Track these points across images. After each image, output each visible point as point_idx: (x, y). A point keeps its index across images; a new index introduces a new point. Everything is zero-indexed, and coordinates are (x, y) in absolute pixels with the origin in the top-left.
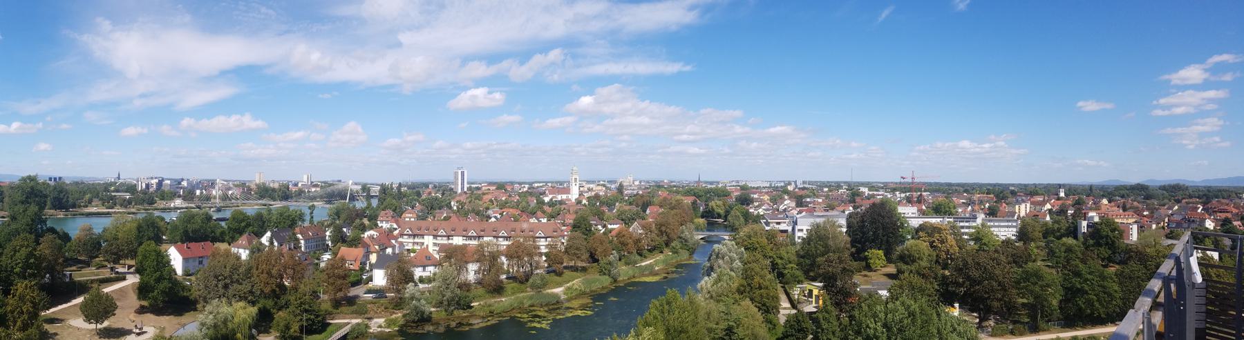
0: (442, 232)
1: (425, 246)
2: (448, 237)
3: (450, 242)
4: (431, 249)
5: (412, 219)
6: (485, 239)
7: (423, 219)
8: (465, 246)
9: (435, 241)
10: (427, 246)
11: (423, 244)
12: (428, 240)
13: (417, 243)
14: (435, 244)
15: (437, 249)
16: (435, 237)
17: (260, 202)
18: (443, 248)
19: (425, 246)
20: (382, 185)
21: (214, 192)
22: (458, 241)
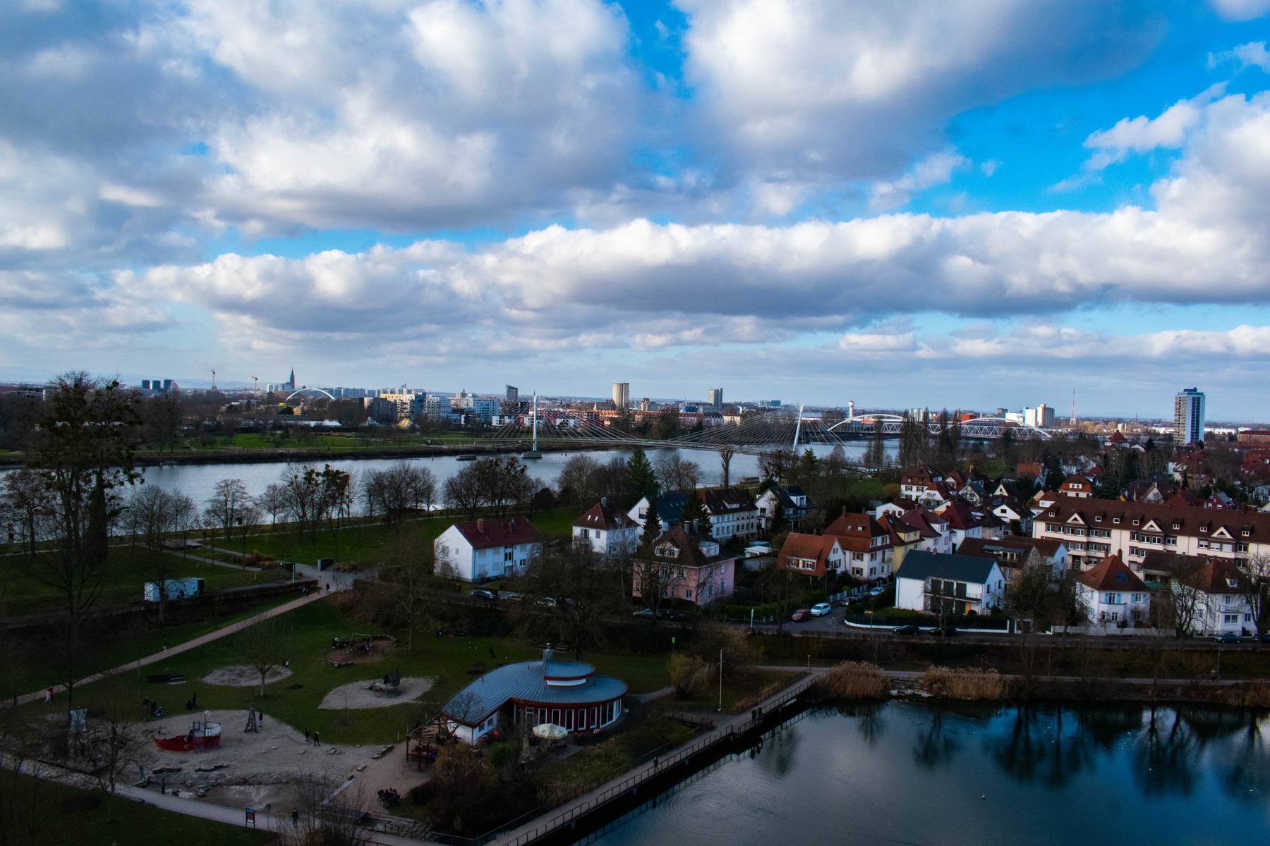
0: (1152, 526)
1: (1114, 552)
2: (1167, 537)
3: (1171, 547)
4: (1126, 559)
5: (1083, 495)
6: (1253, 548)
7: (1107, 497)
8: (1202, 558)
9: (1136, 544)
10: (1120, 552)
11: (1109, 545)
12: (1120, 541)
13: (1099, 546)
14: (1133, 550)
15: (1141, 560)
16: (1137, 534)
17: (624, 441)
18: (1153, 560)
19: (1114, 552)
20: (905, 414)
21: (527, 421)
22: (1187, 546)
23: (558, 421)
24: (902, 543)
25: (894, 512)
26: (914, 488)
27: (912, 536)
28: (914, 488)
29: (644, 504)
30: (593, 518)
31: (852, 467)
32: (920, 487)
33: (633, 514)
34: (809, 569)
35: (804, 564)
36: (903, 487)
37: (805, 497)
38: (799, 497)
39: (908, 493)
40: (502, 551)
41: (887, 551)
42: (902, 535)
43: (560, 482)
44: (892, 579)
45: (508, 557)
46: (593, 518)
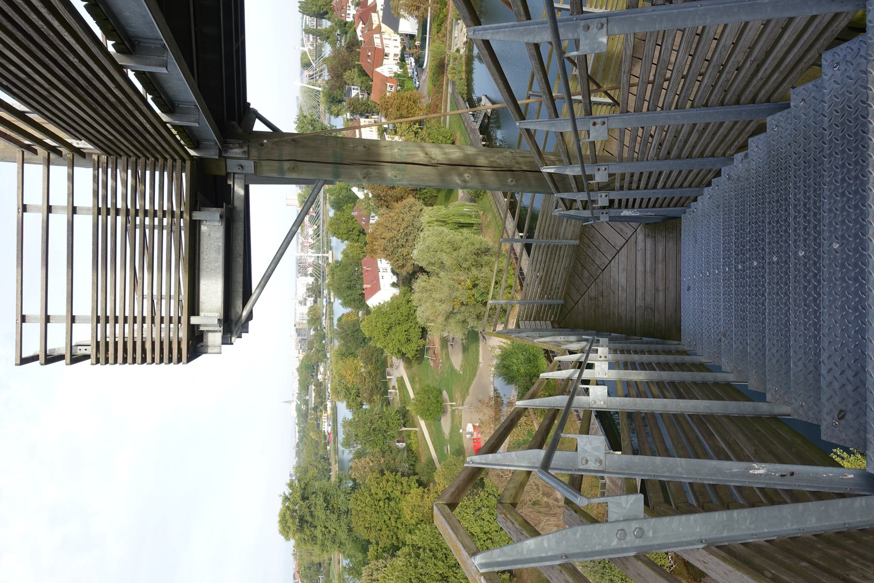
23: (311, 241)
24: (379, 27)
25: (362, 28)
26: (348, 12)
27: (374, 16)
28: (348, 12)
29: (355, 190)
30: (364, 221)
31: (336, 53)
32: (348, 8)
33: (360, 195)
34: (393, 88)
35: (391, 89)
36: (348, 20)
37: (352, 87)
38: (353, 91)
39: (351, 16)
40: (381, 274)
41: (383, 36)
42: (374, 26)
43: (343, 240)
44: (401, 35)
45: (385, 270)
46: (364, 221)
